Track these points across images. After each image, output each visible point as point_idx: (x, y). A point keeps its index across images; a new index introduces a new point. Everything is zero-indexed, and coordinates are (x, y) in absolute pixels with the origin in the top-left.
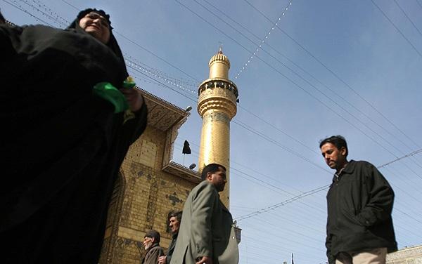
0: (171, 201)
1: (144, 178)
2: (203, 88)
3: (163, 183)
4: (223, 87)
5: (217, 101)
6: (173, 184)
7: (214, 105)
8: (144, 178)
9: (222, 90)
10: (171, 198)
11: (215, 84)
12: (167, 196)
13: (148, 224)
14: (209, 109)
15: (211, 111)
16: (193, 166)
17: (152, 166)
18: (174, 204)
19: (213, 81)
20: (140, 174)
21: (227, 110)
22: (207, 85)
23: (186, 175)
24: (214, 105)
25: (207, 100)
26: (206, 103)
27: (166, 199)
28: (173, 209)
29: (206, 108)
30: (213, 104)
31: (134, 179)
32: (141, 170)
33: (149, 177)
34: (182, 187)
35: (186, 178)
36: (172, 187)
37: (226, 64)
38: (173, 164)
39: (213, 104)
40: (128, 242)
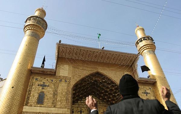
0: (145, 94)
2: (137, 43)
4: (146, 39)
5: (146, 46)
6: (143, 87)
7: (146, 48)
9: (146, 41)
10: (144, 93)
11: (142, 39)
12: (142, 93)
14: (144, 50)
15: (145, 51)
16: (148, 77)
18: (147, 95)
19: (141, 39)
21: (152, 48)
22: (139, 41)
23: (147, 81)
24: (146, 48)
25: (142, 47)
26: (142, 49)
27: (143, 94)
28: (147, 97)
29: (142, 51)
30: (145, 47)
34: (147, 87)
35: (148, 82)
37: (143, 30)
38: (140, 78)
39: (145, 47)
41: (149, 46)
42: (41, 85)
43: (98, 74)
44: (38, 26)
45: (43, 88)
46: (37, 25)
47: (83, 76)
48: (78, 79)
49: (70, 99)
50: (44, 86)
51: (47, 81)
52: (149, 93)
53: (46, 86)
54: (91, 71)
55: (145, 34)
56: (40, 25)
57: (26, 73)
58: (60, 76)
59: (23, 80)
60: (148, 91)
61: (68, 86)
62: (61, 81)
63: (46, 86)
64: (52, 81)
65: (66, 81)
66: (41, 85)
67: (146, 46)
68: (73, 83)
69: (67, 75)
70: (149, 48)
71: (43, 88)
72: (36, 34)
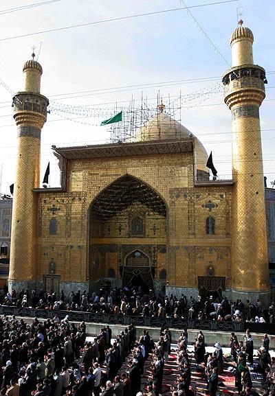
0: (208, 209)
1: (182, 199)
3: (198, 197)
8: (182, 199)
13: (190, 231)
15: (236, 106)
17: (186, 186)
20: (178, 196)
24: (237, 100)
26: (229, 99)
29: (232, 102)
30: (232, 100)
31: (173, 202)
32: (177, 193)
33: (185, 196)
36: (206, 197)
39: (232, 100)
40: (178, 248)
41: (243, 96)
42: (51, 210)
43: (128, 178)
44: (31, 109)
45: (54, 214)
46: (26, 112)
47: (103, 187)
48: (95, 193)
49: (86, 225)
50: (54, 210)
51: (57, 201)
52: (217, 206)
53: (56, 209)
54: (115, 175)
55: (247, 52)
56: (31, 110)
57: (30, 197)
58: (72, 193)
59: (30, 205)
60: (216, 201)
61: (83, 207)
62: (74, 199)
63: (56, 209)
64: (63, 201)
65: (80, 199)
66: (51, 210)
67: (234, 97)
68: (89, 200)
69: (81, 190)
70: (239, 102)
71: (54, 214)
72: (30, 128)
